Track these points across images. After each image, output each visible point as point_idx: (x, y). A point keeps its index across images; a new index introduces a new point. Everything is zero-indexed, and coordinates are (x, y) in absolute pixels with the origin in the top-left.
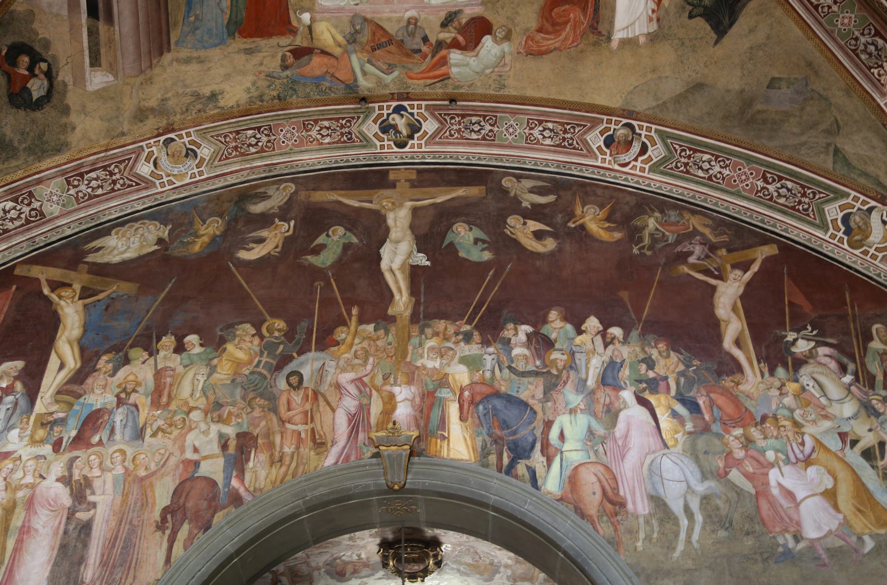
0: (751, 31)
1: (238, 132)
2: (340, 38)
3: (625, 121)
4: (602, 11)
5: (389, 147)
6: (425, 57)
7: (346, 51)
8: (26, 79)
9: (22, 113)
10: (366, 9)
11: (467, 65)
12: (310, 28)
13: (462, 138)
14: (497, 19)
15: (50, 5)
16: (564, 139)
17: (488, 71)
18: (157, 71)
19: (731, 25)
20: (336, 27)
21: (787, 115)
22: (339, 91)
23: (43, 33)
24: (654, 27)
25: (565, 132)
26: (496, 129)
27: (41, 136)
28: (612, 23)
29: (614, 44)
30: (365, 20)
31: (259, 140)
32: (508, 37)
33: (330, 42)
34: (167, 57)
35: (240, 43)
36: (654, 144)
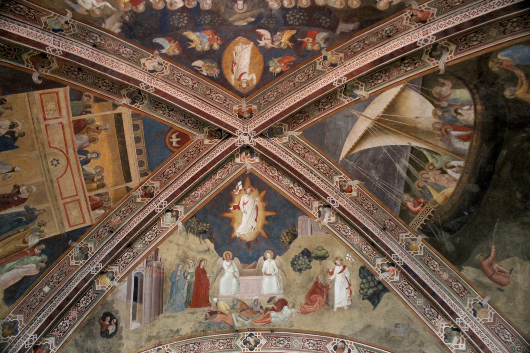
0: (386, 305)
1: (186, 345)
2: (228, 307)
3: (341, 340)
4: (329, 297)
5: (247, 350)
6: (261, 314)
7: (230, 312)
8: (108, 326)
9: (105, 339)
10: (239, 296)
11: (278, 317)
12: (217, 304)
13: (276, 346)
14: (289, 300)
15: (120, 297)
16: (317, 347)
17: (286, 320)
18: (157, 321)
19: (378, 303)
20: (227, 303)
21: (403, 338)
22: (228, 328)
23: (116, 308)
24: (350, 303)
25: (318, 344)
26: (290, 343)
27: (110, 349)
28: (333, 301)
29: (335, 309)
30: (238, 300)
31: (194, 348)
32: (293, 307)
33: (224, 309)
34: (161, 316)
35: (189, 310)
36: (353, 349)
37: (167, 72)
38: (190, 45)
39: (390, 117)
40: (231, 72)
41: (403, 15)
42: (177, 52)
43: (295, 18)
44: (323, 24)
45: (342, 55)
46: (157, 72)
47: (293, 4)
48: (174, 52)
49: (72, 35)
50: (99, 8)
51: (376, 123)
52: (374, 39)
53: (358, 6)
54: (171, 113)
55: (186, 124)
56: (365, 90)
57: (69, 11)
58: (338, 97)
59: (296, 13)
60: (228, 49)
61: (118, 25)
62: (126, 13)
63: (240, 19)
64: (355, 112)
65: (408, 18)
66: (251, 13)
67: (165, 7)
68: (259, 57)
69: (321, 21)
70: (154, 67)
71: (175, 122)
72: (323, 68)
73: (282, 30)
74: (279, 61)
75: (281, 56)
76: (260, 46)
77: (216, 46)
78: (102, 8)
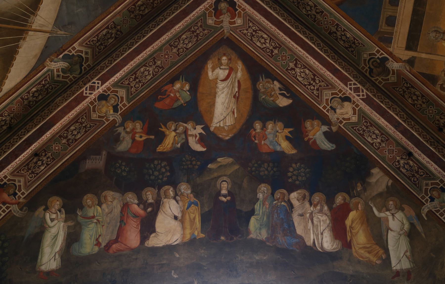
37: (326, 95)
38: (289, 132)
39: (6, 42)
40: (242, 83)
41: (26, 194)
42: (308, 124)
43: (159, 171)
44: (124, 164)
45: (94, 116)
46: (340, 98)
47: (162, 192)
48: (312, 126)
49: (433, 179)
50: (388, 210)
51: (25, 26)
52: (56, 147)
53: (85, 197)
54: (334, 29)
55: (315, 6)
56: (52, 71)
57: (424, 215)
58: (89, 51)
59: (159, 179)
60: (243, 121)
61: (373, 180)
62: (359, 196)
63: (225, 166)
64: (61, 33)
65: (20, 190)
66: (212, 176)
67: (311, 195)
68: (203, 106)
69: (127, 169)
70: (342, 107)
71: (331, 14)
72: (117, 92)
73: (174, 151)
74: (177, 99)
75: (174, 109)
76: (201, 125)
77: (258, 126)
78: (384, 209)
